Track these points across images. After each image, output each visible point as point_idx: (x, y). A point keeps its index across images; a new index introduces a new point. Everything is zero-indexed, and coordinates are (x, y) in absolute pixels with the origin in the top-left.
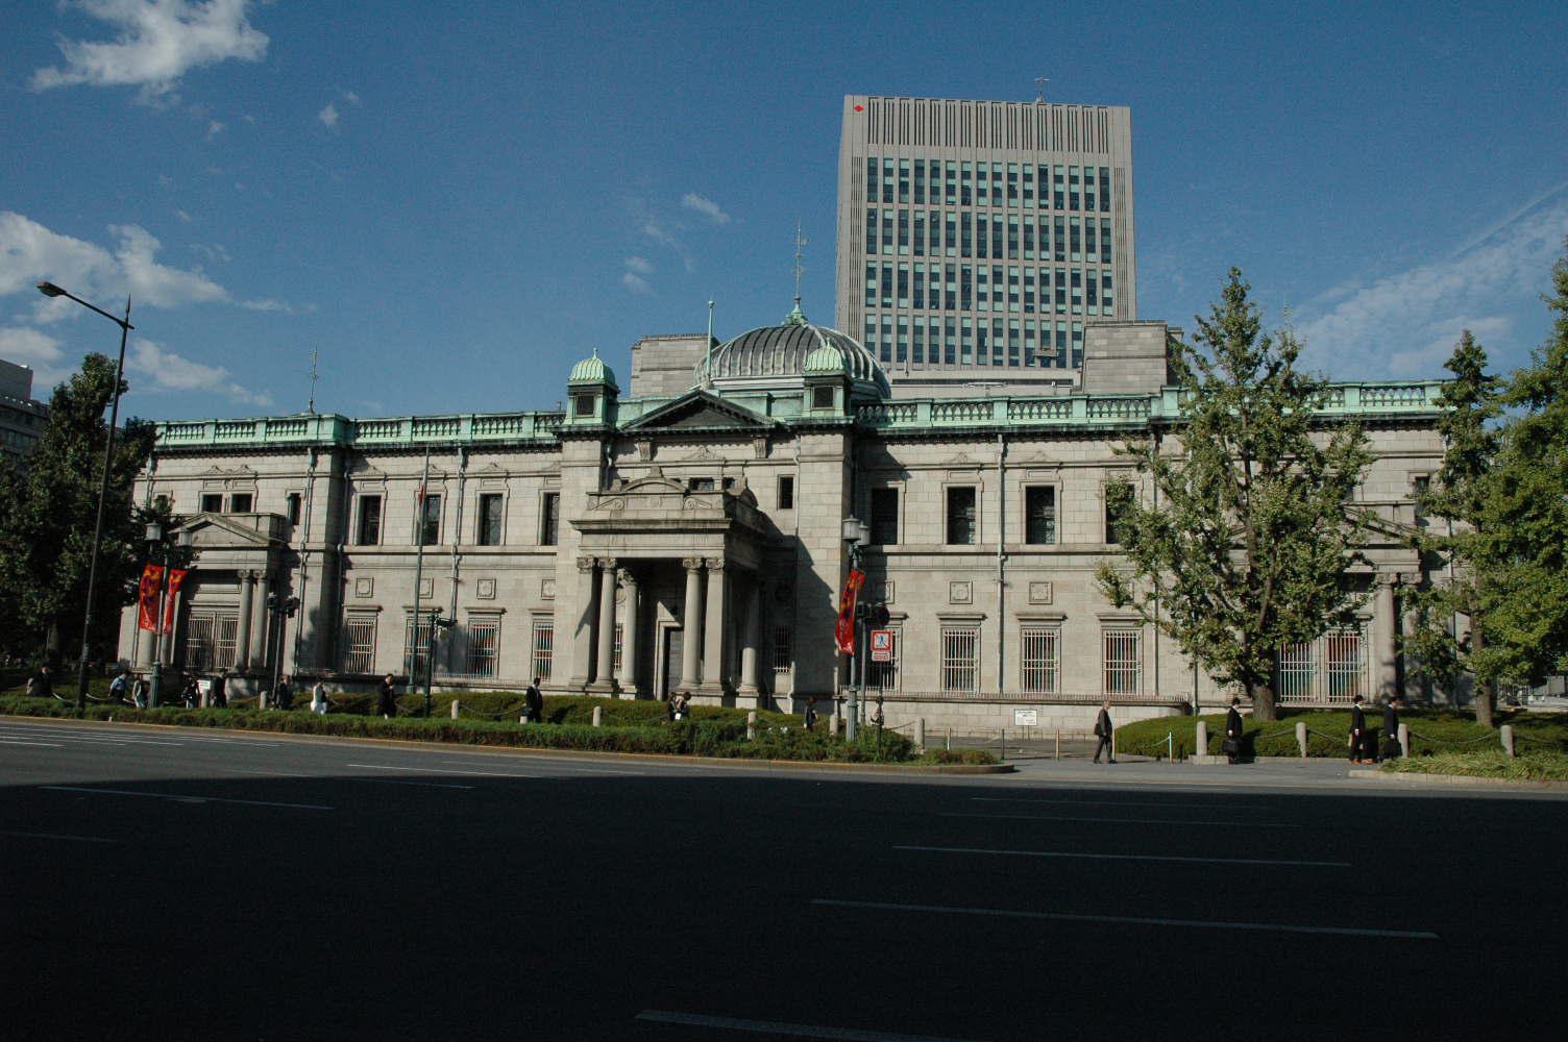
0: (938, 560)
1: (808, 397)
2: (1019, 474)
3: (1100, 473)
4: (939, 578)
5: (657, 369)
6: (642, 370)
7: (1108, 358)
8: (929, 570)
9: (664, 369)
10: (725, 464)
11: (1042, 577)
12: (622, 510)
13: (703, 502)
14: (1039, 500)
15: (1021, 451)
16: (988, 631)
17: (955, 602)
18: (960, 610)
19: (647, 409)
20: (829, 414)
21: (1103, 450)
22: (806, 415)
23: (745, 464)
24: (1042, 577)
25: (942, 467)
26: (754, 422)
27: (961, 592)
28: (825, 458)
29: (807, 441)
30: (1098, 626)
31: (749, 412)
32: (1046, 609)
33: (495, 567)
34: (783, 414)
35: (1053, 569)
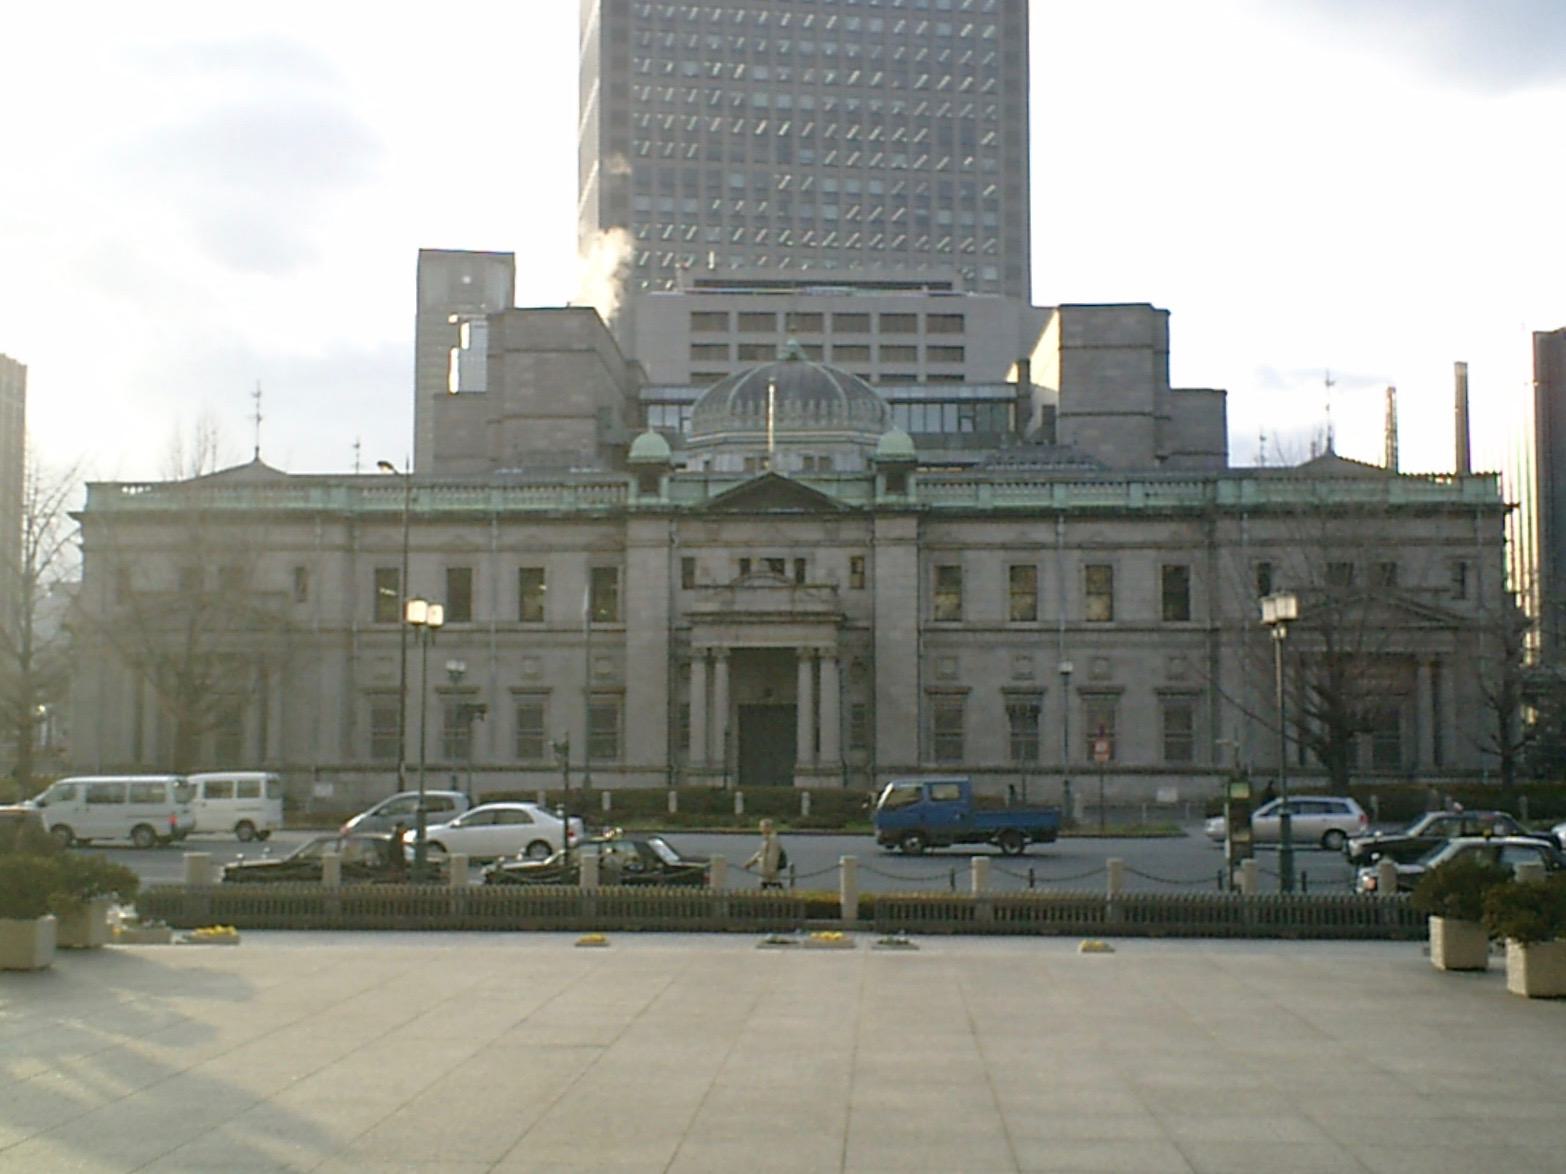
0: (1001, 637)
1: (881, 482)
2: (1077, 554)
3: (1152, 553)
4: (1002, 653)
5: (527, 350)
6: (509, 351)
7: (1084, 347)
8: (991, 647)
9: (536, 351)
10: (797, 544)
11: (1103, 652)
12: (733, 602)
13: (811, 595)
14: (1101, 581)
15: (1084, 531)
16: (1049, 704)
17: (1019, 677)
18: (1025, 684)
19: (714, 491)
20: (902, 500)
21: (1161, 532)
22: (880, 500)
23: (817, 544)
24: (1103, 652)
25: (1004, 547)
26: (830, 506)
27: (1024, 667)
28: (899, 541)
29: (882, 527)
30: (1152, 700)
31: (824, 496)
32: (1106, 683)
33: (540, 644)
34: (853, 497)
35: (1113, 645)
